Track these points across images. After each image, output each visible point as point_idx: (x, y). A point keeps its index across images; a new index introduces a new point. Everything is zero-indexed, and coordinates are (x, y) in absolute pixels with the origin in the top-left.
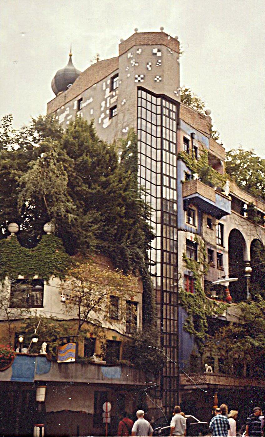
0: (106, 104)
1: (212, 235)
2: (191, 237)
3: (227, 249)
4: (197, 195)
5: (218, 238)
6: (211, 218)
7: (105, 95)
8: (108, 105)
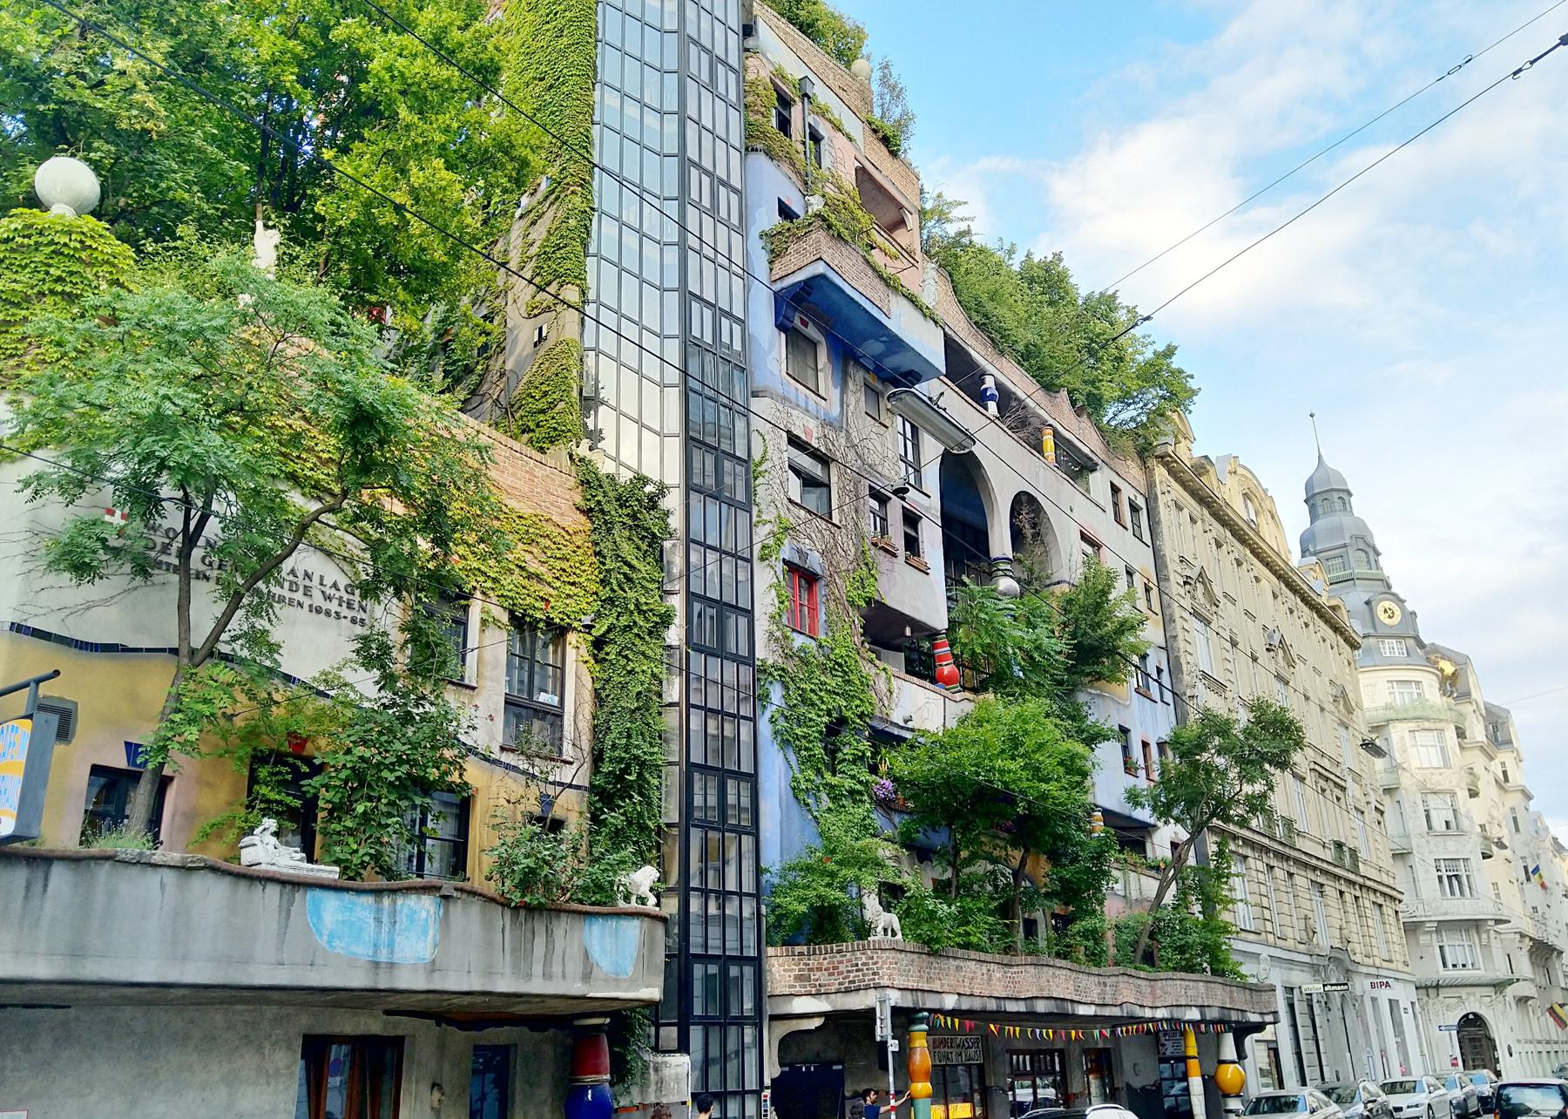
4: (820, 268)
5: (904, 459)
6: (879, 386)
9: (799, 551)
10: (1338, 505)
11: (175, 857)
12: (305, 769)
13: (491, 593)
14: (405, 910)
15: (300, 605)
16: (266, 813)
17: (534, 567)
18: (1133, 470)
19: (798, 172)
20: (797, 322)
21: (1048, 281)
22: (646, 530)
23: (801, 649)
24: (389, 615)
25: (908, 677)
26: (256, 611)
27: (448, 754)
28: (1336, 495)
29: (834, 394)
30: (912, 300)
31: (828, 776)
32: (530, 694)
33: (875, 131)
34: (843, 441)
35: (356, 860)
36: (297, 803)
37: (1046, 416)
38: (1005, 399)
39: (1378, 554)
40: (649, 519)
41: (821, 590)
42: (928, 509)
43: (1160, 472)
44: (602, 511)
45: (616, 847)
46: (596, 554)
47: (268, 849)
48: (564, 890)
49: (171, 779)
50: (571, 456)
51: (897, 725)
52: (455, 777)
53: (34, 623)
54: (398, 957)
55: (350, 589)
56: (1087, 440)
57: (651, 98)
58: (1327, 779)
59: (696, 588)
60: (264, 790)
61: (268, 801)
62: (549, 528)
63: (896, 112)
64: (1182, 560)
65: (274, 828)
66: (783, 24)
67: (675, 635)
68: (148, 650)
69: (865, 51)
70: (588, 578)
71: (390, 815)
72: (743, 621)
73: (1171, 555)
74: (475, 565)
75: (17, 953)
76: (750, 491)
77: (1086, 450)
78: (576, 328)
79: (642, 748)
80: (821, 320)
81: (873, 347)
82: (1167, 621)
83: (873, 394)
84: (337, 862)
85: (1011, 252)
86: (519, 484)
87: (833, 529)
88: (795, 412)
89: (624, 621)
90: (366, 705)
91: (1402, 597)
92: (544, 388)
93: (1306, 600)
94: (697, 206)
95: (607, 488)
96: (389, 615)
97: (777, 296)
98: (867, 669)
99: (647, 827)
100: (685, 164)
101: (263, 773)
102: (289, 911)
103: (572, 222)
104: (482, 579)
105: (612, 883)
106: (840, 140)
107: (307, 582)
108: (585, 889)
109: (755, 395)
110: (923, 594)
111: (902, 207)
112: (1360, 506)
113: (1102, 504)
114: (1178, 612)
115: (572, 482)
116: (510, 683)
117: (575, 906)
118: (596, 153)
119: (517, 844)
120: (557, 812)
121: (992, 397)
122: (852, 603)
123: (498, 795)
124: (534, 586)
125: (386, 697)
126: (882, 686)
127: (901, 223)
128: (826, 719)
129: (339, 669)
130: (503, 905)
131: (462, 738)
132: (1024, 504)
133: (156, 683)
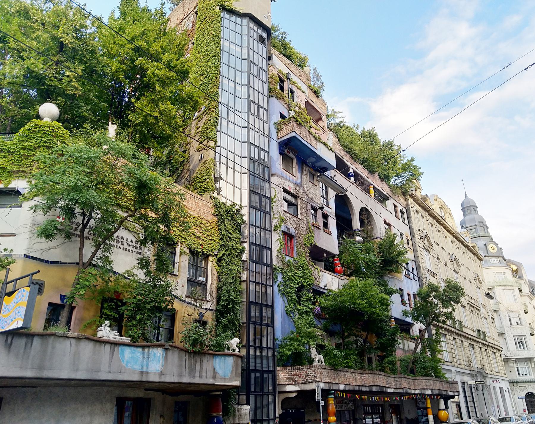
1: (315, 192)
2: (290, 187)
4: (294, 134)
5: (322, 196)
6: (314, 172)
9: (287, 228)
10: (473, 211)
11: (75, 334)
12: (120, 304)
13: (184, 243)
14: (153, 353)
15: (120, 248)
16: (106, 319)
17: (198, 234)
18: (401, 200)
19: (286, 104)
20: (286, 152)
21: (370, 137)
22: (236, 221)
23: (289, 261)
24: (149, 251)
25: (325, 271)
26: (105, 250)
27: (168, 298)
28: (472, 208)
29: (299, 175)
30: (325, 144)
31: (298, 306)
32: (196, 278)
33: (312, 90)
34: (302, 191)
35: (136, 336)
36: (117, 316)
37: (371, 182)
38: (357, 176)
39: (488, 228)
40: (237, 218)
41: (295, 241)
42: (331, 213)
43: (411, 200)
44: (221, 215)
45: (225, 331)
46: (219, 229)
47: (106, 332)
48: (207, 346)
49: (75, 307)
50: (211, 197)
51: (321, 288)
52: (170, 306)
53: (31, 255)
54: (150, 370)
55: (136, 242)
56: (385, 189)
57: (238, 80)
58: (473, 307)
59: (252, 240)
60: (106, 311)
61: (107, 315)
62: (203, 221)
63: (319, 83)
64: (419, 230)
65: (109, 325)
66: (281, 56)
67: (245, 257)
68: (69, 263)
69: (308, 64)
70: (216, 238)
71: (148, 320)
72: (268, 252)
74: (178, 234)
75: (21, 368)
76: (271, 208)
77: (385, 193)
78: (213, 155)
79: (234, 296)
80: (295, 152)
81: (313, 160)
82: (415, 251)
83: (312, 175)
84: (130, 336)
85: (357, 128)
86: (193, 206)
87: (299, 220)
88: (286, 181)
89: (228, 252)
90: (141, 282)
91: (497, 243)
92: (202, 175)
93: (463, 244)
94: (253, 115)
95: (223, 207)
96: (149, 251)
97: (279, 143)
98: (311, 268)
99: (235, 324)
100: (249, 101)
101: (106, 305)
102: (113, 354)
103: (212, 121)
104: (180, 238)
105: (223, 344)
106: (300, 93)
107: (122, 240)
108: (214, 346)
109: (272, 175)
110: (330, 242)
111: (321, 114)
112: (481, 211)
113: (391, 211)
114: (418, 248)
115: (211, 205)
116: (189, 274)
117: (211, 352)
118: (220, 98)
119: (191, 330)
120: (205, 318)
121: (352, 176)
122: (306, 246)
123: (184, 312)
124: (198, 241)
125: (148, 278)
126: (317, 274)
127: (321, 119)
128: (297, 286)
129: (132, 269)
130: (186, 351)
131: (173, 293)
132: (364, 211)
133: (71, 275)
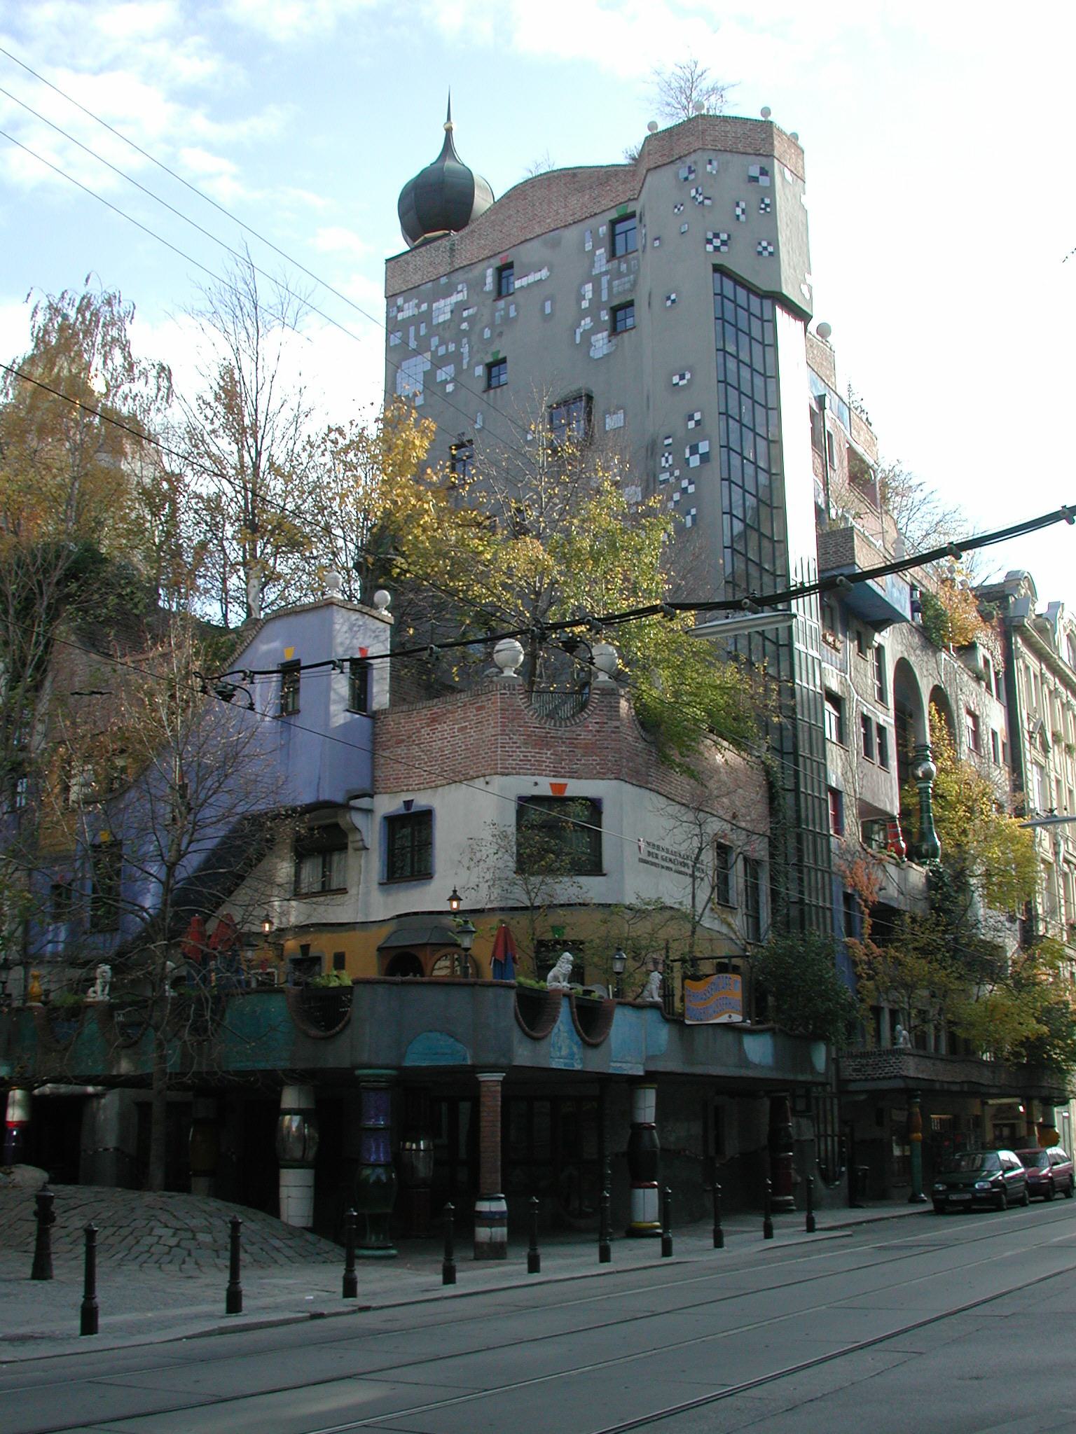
0: (597, 291)
3: (892, 713)
6: (862, 630)
7: (592, 265)
8: (605, 298)
43: (1018, 641)
73: (1023, 713)
